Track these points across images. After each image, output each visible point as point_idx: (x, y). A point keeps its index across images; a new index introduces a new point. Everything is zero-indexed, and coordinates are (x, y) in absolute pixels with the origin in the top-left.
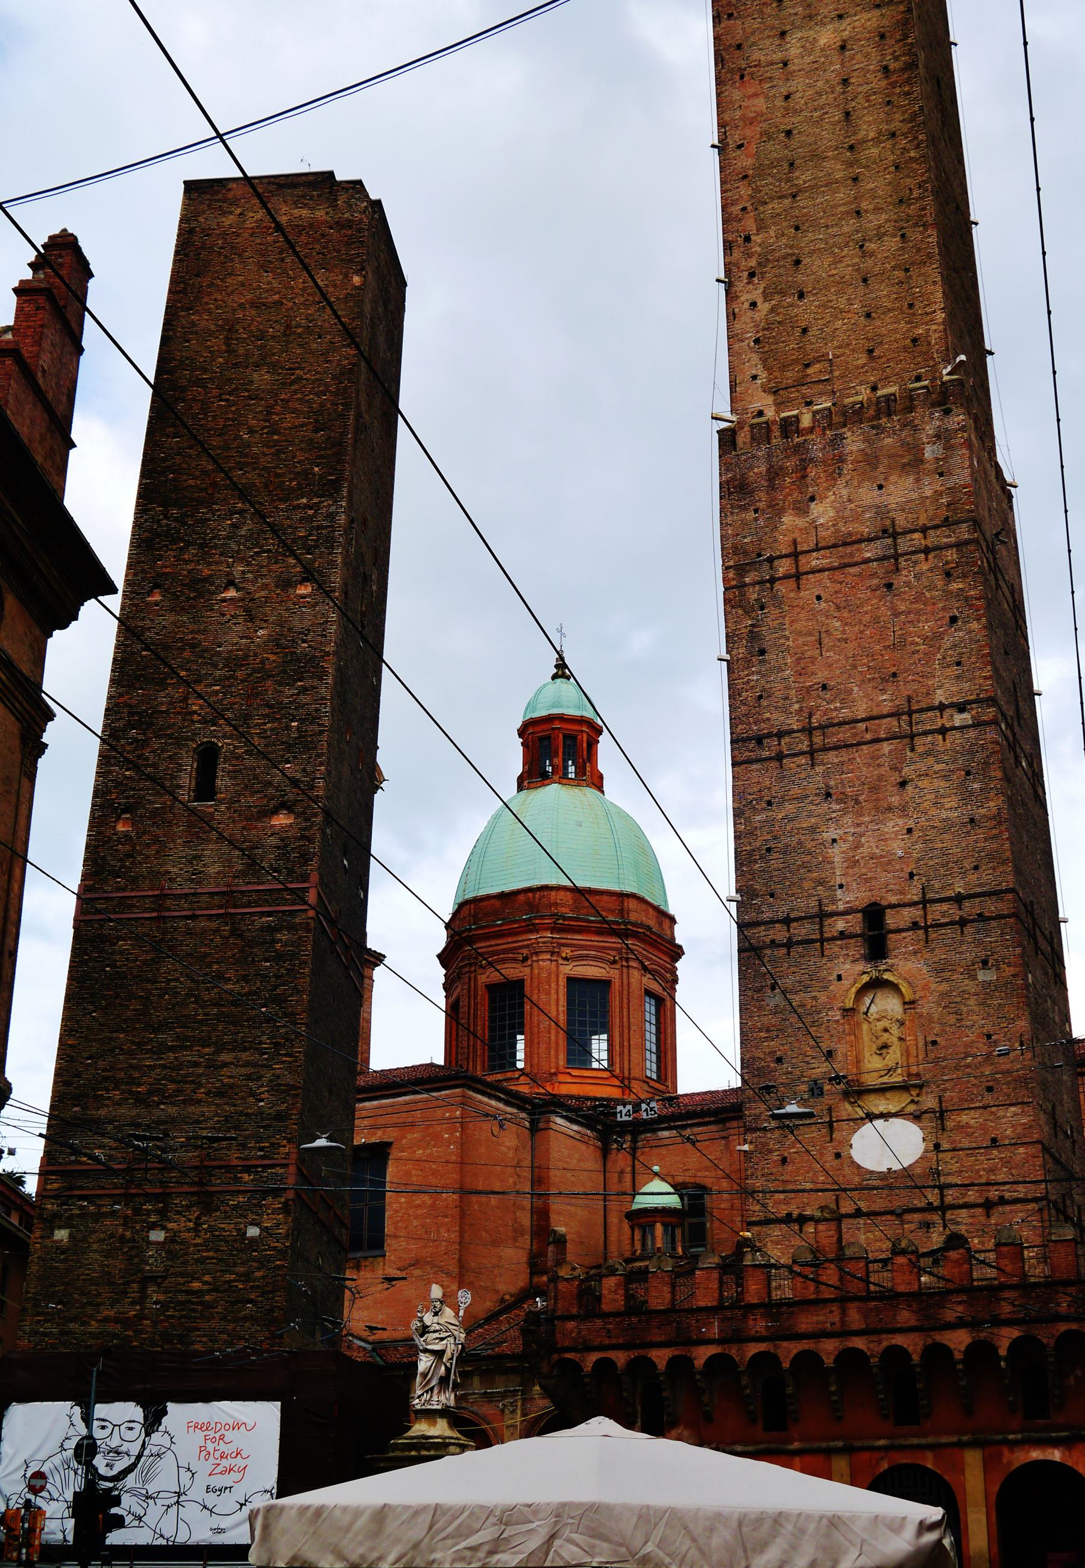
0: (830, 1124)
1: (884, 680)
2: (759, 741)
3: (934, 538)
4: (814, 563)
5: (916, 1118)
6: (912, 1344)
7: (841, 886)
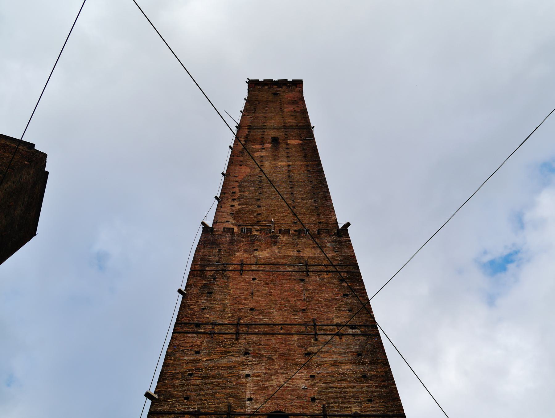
1: (295, 311)
2: (198, 325)
4: (253, 268)
7: (250, 399)
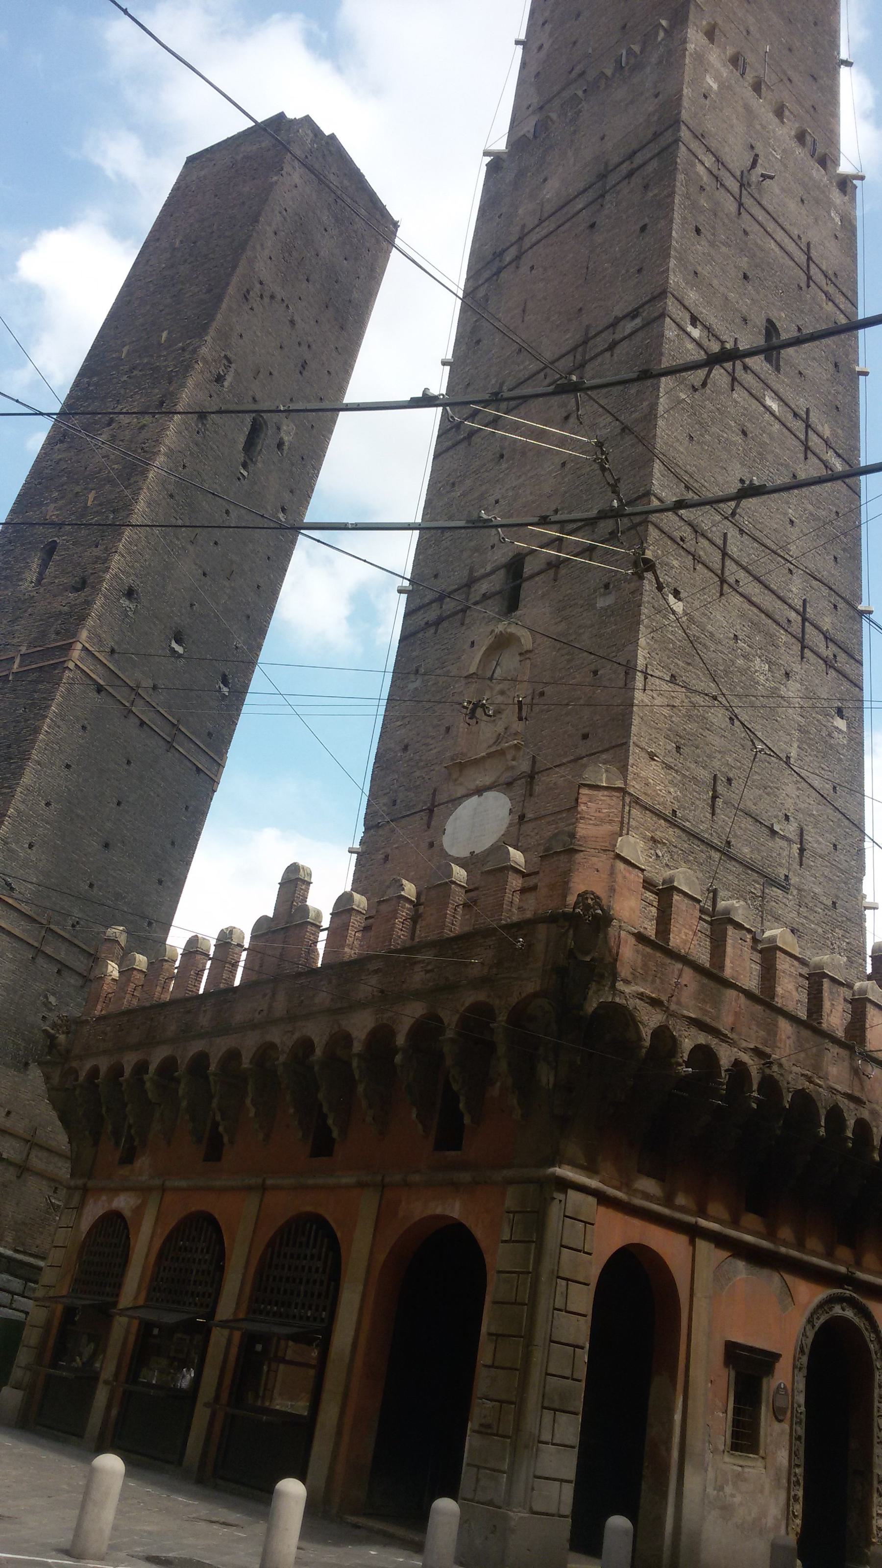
0: (431, 811)
3: (638, 160)
5: (507, 786)
6: (318, 1032)
